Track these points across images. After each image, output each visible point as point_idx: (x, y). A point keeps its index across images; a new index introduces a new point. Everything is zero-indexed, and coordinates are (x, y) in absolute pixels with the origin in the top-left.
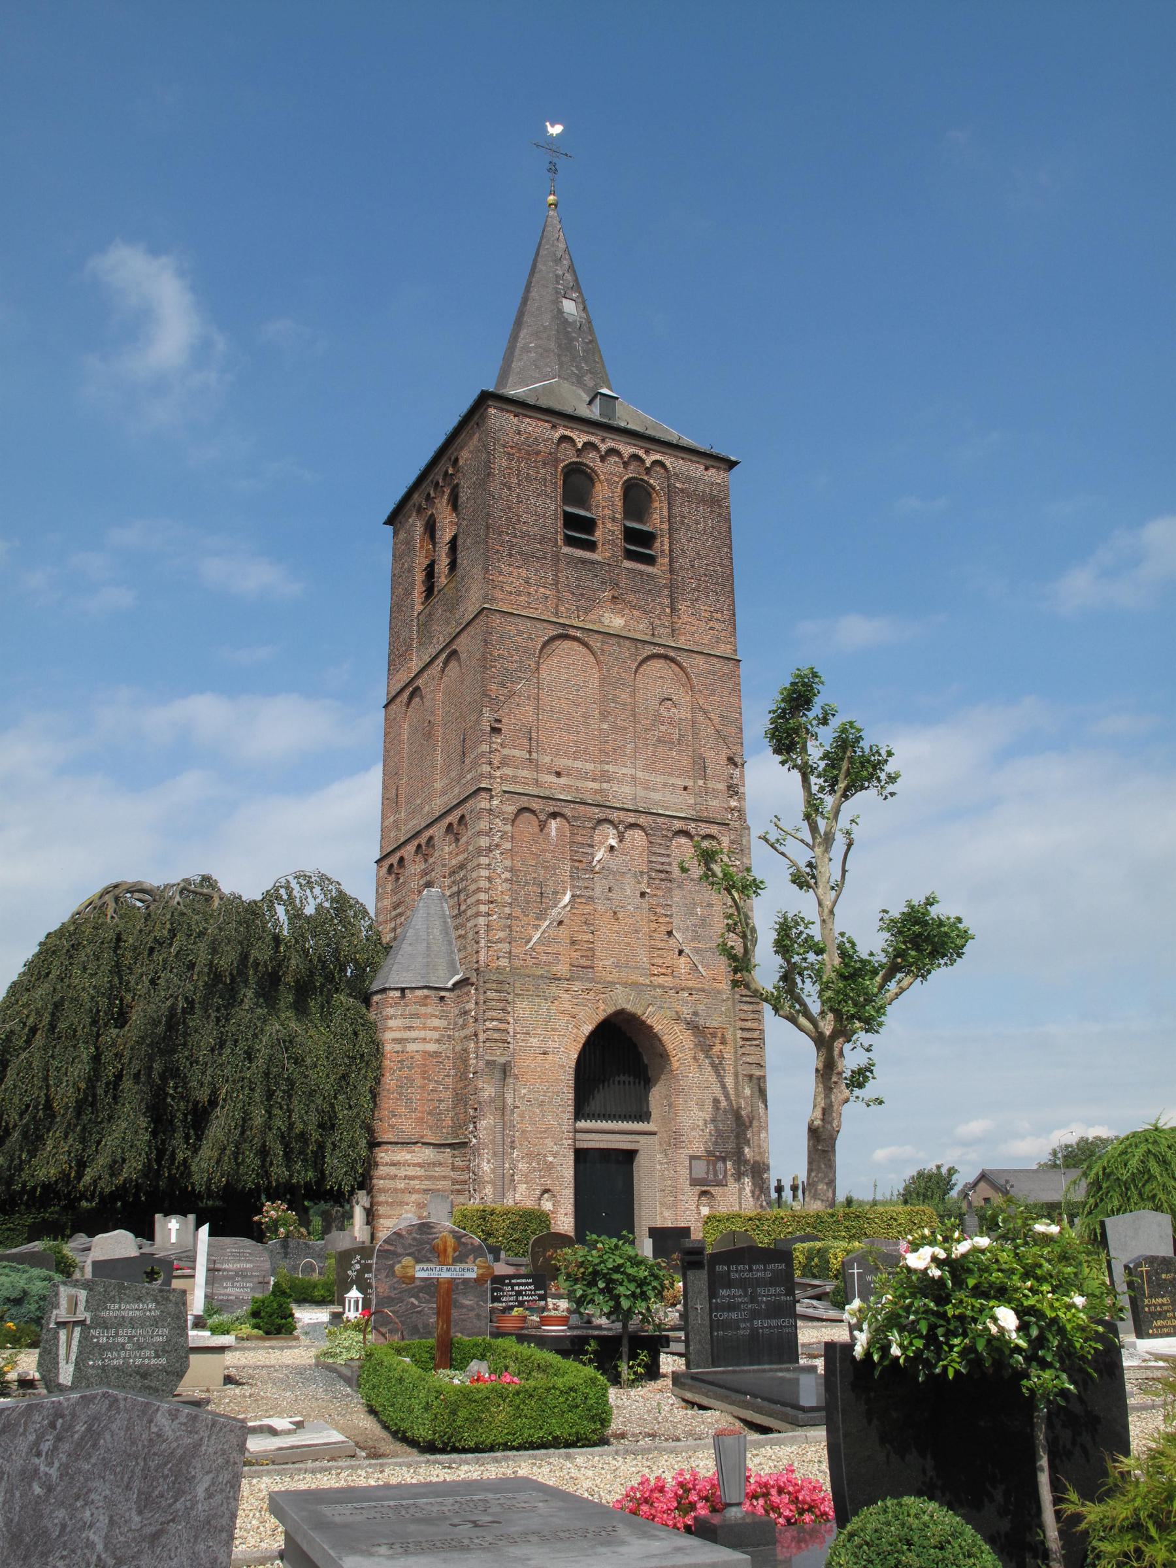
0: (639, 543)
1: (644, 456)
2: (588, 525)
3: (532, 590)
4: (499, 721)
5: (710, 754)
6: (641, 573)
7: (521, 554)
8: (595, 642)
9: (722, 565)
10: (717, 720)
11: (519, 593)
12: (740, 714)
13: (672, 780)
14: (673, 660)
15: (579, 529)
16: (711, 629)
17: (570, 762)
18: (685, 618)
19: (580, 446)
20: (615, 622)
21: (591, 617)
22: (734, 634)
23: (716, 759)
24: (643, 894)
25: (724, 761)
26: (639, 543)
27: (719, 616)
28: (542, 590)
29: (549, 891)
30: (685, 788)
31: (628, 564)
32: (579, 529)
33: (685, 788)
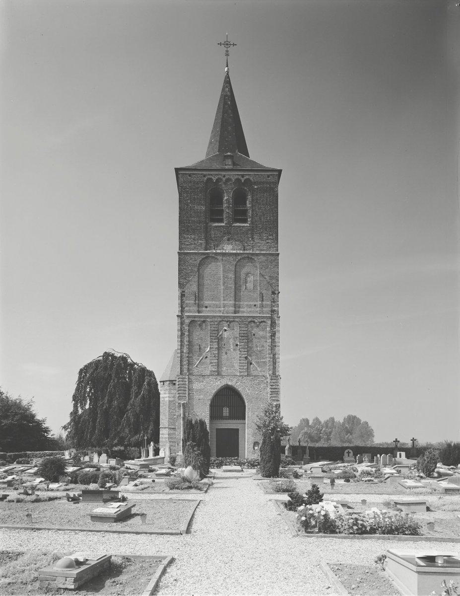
3: (196, 242)
4: (183, 292)
5: (264, 292)
6: (240, 226)
11: (191, 244)
12: (278, 274)
13: (251, 303)
14: (252, 258)
16: (268, 243)
17: (210, 302)
20: (228, 248)
21: (220, 247)
22: (277, 243)
23: (267, 294)
24: (237, 345)
25: (270, 292)
28: (200, 241)
29: (202, 347)
30: (255, 306)
33: (255, 306)
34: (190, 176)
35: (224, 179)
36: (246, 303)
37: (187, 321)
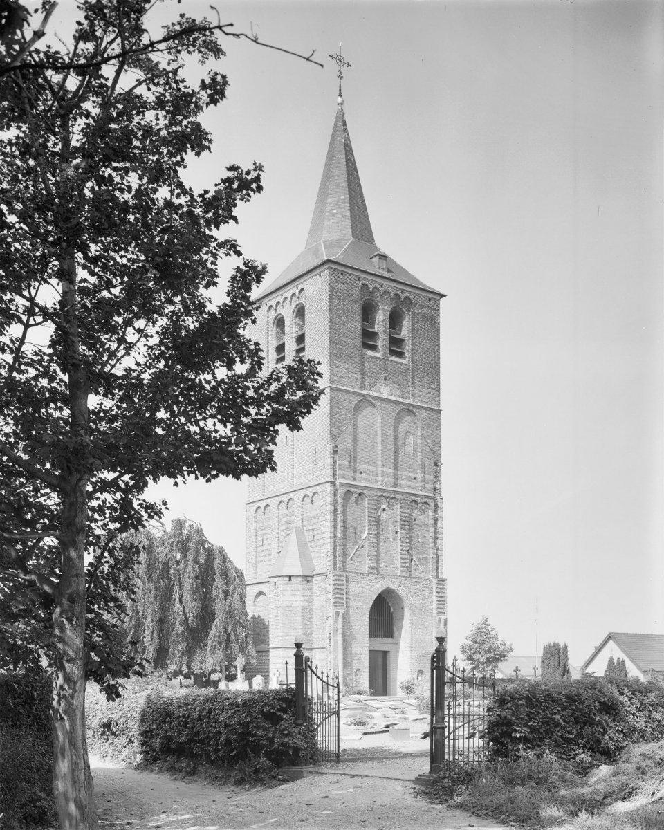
0: (396, 345)
1: (401, 294)
2: (373, 335)
4: (336, 446)
6: (397, 363)
7: (345, 355)
8: (376, 402)
9: (435, 357)
10: (430, 443)
11: (344, 377)
15: (368, 338)
17: (366, 467)
18: (418, 388)
19: (371, 290)
26: (396, 345)
27: (432, 386)
28: (354, 375)
29: (358, 531)
31: (393, 358)
32: (368, 338)
34: (342, 274)
35: (382, 290)
36: (405, 474)
37: (341, 491)
